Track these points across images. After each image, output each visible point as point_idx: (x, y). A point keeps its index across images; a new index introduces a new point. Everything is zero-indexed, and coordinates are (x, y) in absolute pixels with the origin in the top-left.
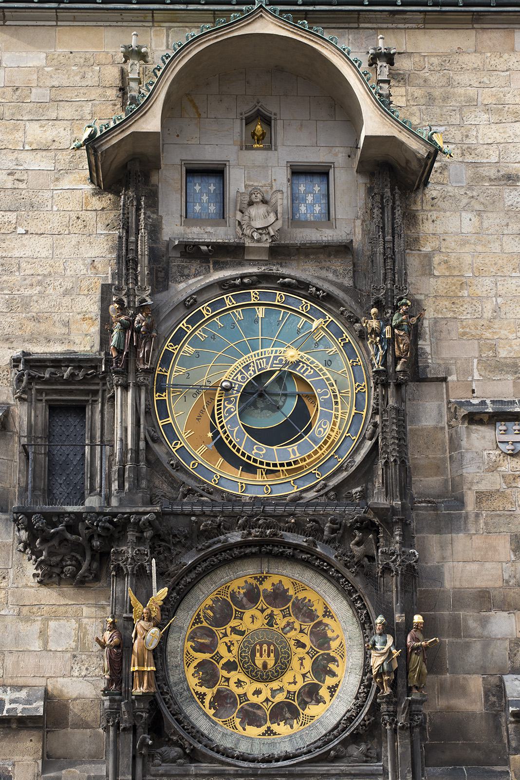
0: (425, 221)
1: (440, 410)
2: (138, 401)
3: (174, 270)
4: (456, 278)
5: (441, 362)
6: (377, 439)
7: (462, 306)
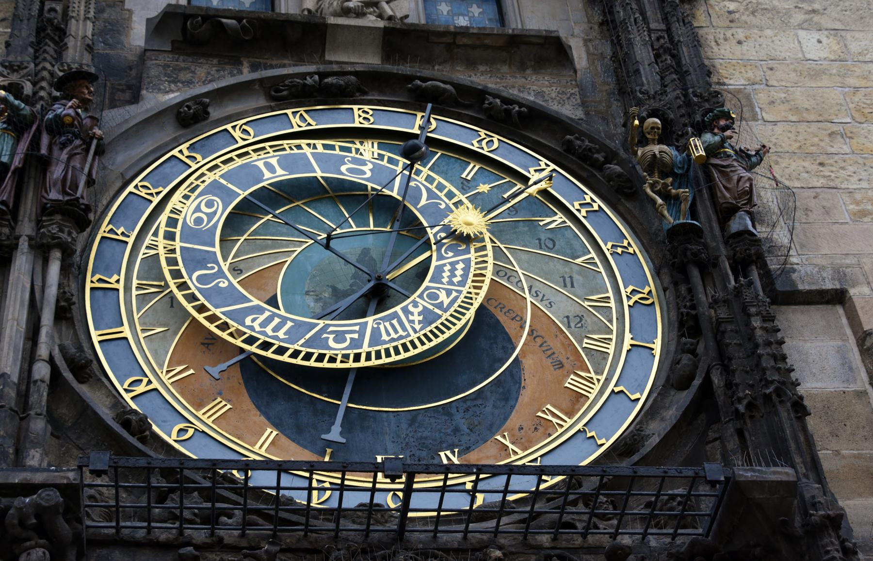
0: (721, 41)
1: (843, 357)
2: (38, 283)
3: (153, 72)
4: (814, 127)
5: (823, 262)
6: (707, 380)
7: (843, 168)
